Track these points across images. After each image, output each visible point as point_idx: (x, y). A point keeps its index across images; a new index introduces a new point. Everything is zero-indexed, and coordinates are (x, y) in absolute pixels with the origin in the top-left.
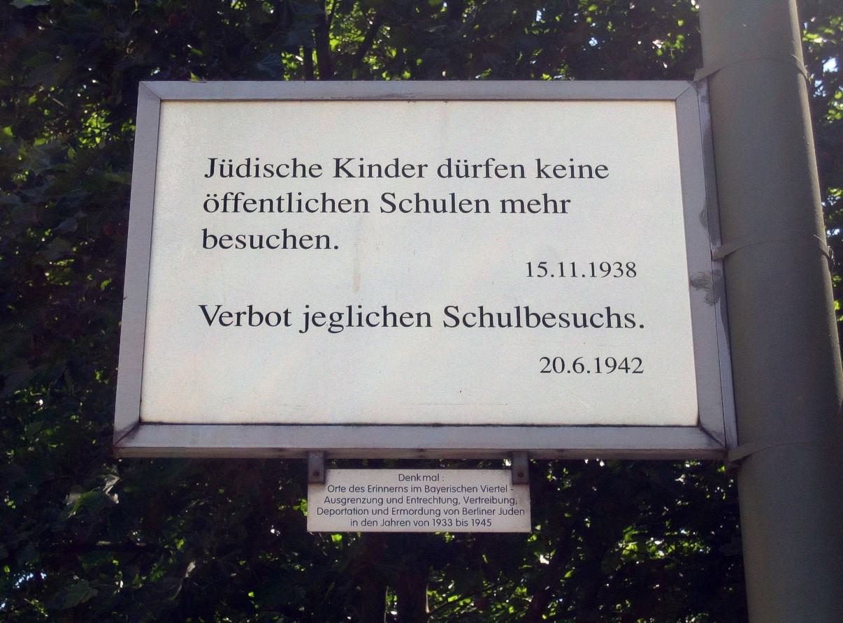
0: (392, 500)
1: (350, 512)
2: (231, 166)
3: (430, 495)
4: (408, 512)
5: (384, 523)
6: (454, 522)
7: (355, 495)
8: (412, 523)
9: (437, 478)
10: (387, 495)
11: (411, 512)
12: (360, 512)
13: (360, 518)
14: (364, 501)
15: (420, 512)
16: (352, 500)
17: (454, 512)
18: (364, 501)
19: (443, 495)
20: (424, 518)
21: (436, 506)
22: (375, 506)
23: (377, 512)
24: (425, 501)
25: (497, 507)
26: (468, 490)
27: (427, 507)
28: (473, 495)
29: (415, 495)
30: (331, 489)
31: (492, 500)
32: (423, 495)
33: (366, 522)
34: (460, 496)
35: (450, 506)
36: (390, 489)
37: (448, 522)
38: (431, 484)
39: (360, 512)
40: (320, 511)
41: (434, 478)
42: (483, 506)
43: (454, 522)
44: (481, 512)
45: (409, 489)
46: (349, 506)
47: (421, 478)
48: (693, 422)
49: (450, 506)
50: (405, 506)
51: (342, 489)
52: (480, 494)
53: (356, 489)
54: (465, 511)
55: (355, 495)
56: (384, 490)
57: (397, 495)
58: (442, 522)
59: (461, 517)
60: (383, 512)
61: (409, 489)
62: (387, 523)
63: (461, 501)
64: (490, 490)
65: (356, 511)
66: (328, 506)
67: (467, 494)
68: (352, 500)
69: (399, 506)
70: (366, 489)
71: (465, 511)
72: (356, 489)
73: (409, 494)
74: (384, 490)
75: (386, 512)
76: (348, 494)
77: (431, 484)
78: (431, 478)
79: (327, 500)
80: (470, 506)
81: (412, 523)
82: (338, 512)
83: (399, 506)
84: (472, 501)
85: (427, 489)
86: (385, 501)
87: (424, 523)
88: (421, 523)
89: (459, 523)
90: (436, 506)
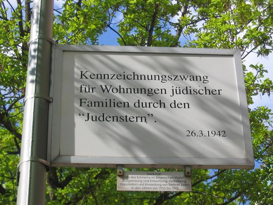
2: (180, 90)
16: (132, 181)
21: (160, 183)
22: (139, 183)
27: (157, 183)
46: (131, 183)
49: (165, 183)
50: (149, 183)
69: (147, 183)
83: (147, 183)
90: (160, 183)
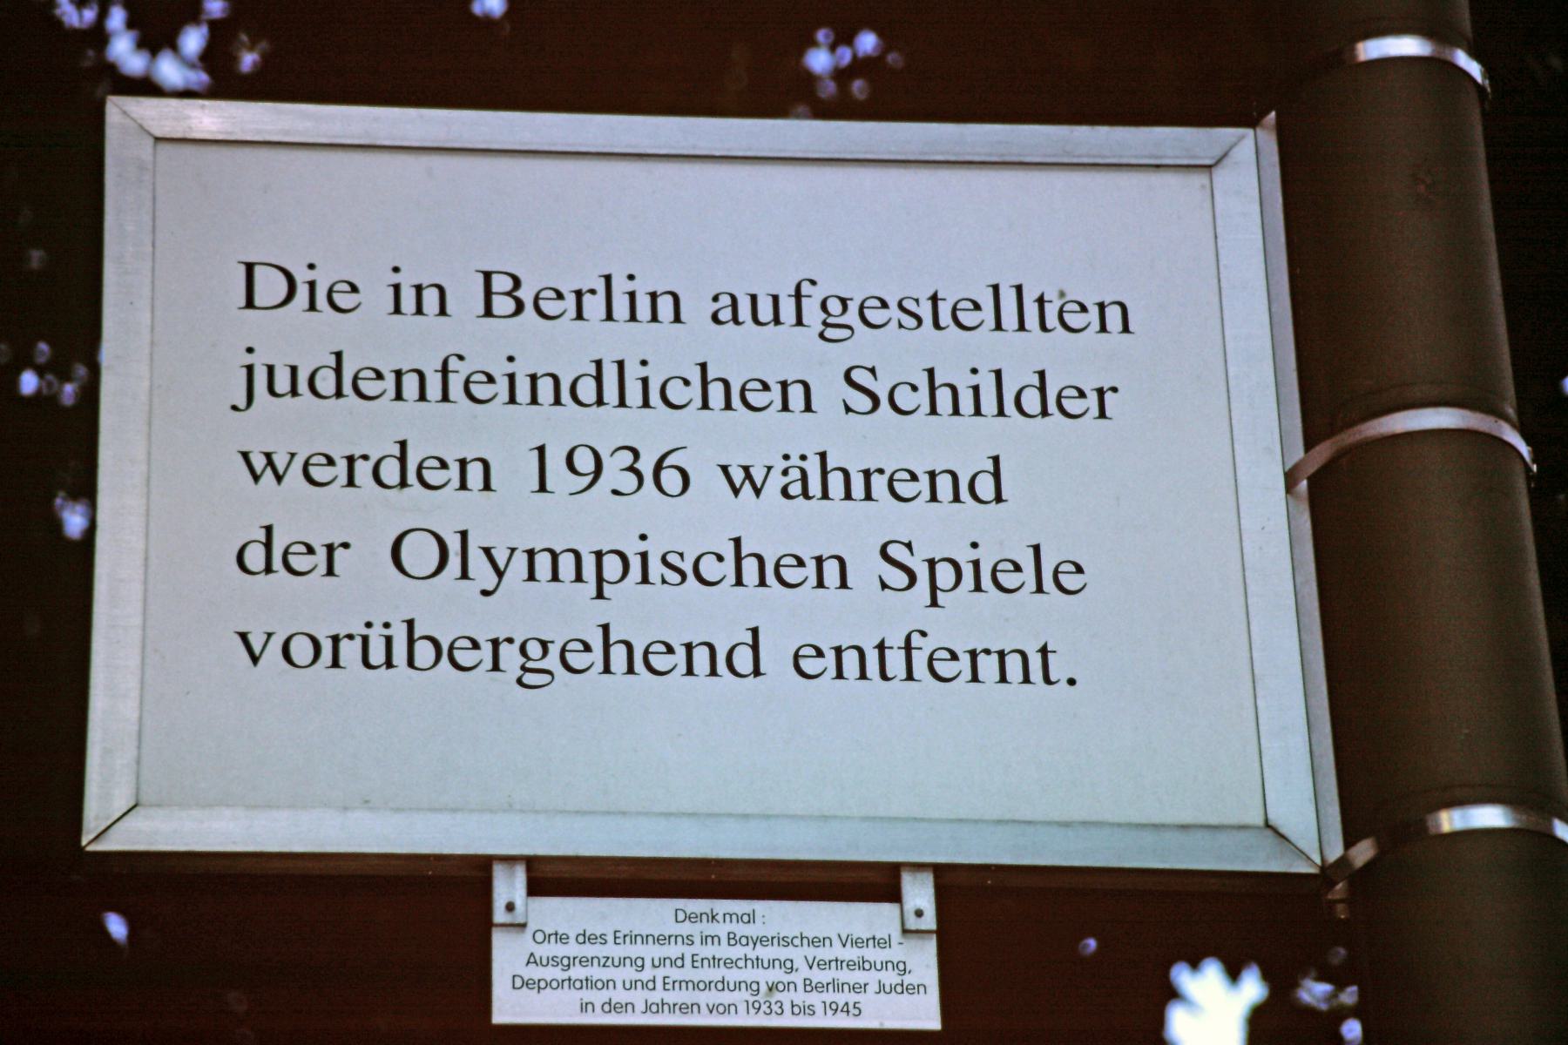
0: (663, 961)
1: (578, 985)
3: (737, 952)
4: (696, 986)
5: (648, 1008)
6: (787, 1007)
7: (589, 950)
8: (704, 1009)
9: (751, 918)
10: (652, 952)
11: (702, 986)
12: (600, 985)
13: (599, 997)
14: (606, 962)
15: (720, 986)
16: (585, 961)
17: (787, 986)
18: (606, 962)
19: (765, 953)
20: (726, 997)
21: (749, 974)
23: (634, 984)
24: (730, 963)
25: (871, 977)
26: (813, 942)
27: (733, 975)
28: (824, 953)
29: (708, 951)
30: (539, 937)
31: (862, 964)
32: (724, 951)
33: (611, 1006)
34: (798, 954)
35: (776, 975)
36: (660, 940)
37: (775, 1008)
38: (741, 929)
39: (600, 985)
40: (518, 983)
41: (746, 918)
42: (845, 976)
43: (787, 1007)
44: (838, 986)
45: (697, 940)
46: (577, 972)
47: (720, 918)
48: (1260, 821)
49: (776, 975)
50: (687, 973)
51: (562, 938)
52: (838, 951)
53: (586, 938)
54: (809, 986)
55: (589, 950)
56: (645, 939)
57: (673, 951)
58: (764, 1008)
59: (800, 997)
60: (644, 986)
61: (697, 940)
62: (654, 1008)
63: (799, 963)
64: (857, 943)
65: (588, 983)
66: (535, 973)
67: (811, 952)
68: (585, 961)
69: (675, 974)
70: (610, 938)
71: (809, 986)
72: (586, 938)
73: (697, 948)
74: (645, 939)
75: (651, 985)
76: (573, 949)
77: (741, 929)
78: (740, 919)
79: (532, 960)
80: (818, 976)
81: (704, 1009)
82: (554, 984)
83: (675, 974)
84: (823, 965)
85: (732, 939)
86: (648, 963)
87: (727, 1009)
88: (721, 1009)
89: (796, 1010)
90: (749, 974)
